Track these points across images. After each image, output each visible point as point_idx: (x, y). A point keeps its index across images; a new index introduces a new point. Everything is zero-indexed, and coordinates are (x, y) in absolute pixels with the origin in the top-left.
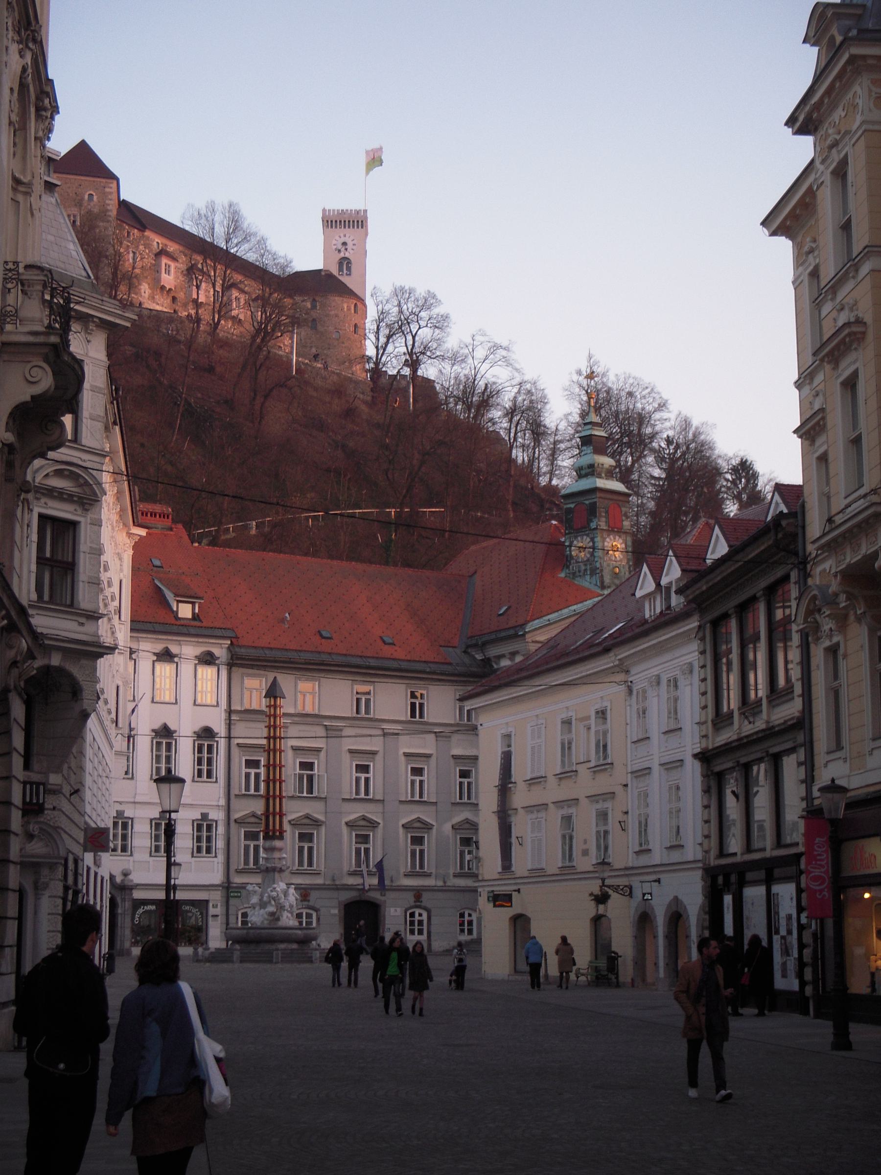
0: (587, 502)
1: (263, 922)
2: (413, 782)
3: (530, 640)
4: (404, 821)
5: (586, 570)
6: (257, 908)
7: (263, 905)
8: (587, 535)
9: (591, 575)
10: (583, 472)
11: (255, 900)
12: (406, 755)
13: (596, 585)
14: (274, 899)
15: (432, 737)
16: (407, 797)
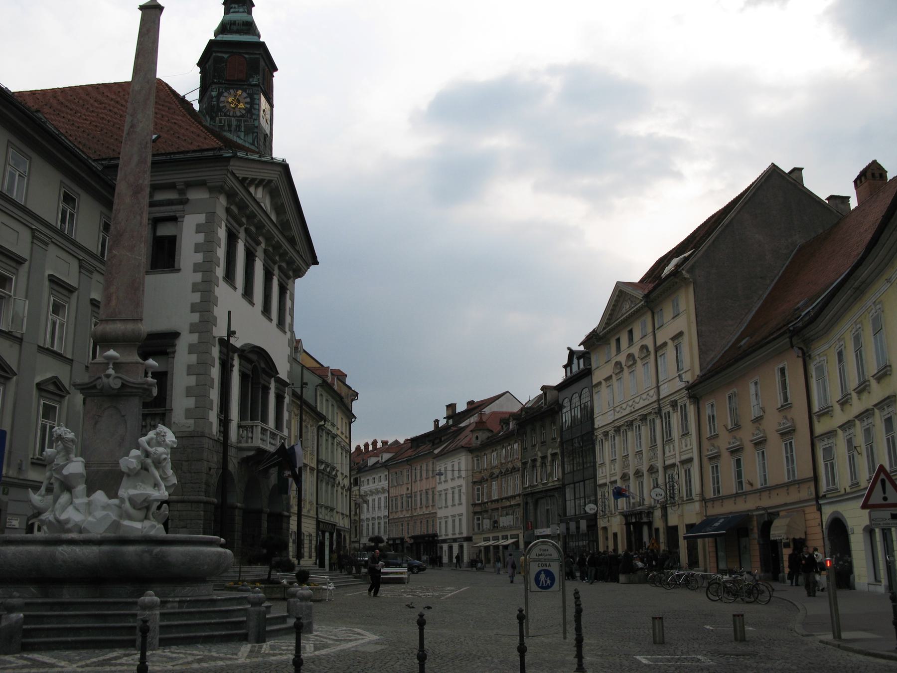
0: (246, 56)
1: (116, 525)
2: (54, 324)
3: (230, 168)
4: (38, 379)
5: (238, 127)
6: (81, 488)
7: (106, 479)
8: (244, 90)
9: (246, 134)
10: (235, 28)
11: (76, 466)
12: (53, 279)
13: (253, 144)
14: (158, 463)
15: (75, 264)
16: (45, 343)
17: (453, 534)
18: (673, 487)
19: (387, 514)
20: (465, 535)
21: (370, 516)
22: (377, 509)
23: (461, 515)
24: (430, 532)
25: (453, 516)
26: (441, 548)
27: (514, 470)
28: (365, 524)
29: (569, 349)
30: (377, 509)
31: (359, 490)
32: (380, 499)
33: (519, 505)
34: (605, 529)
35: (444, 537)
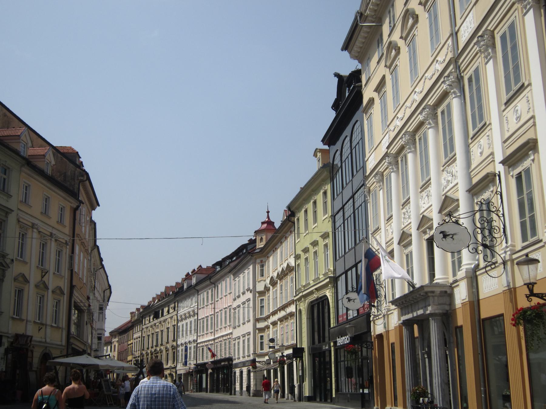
17: (244, 357)
18: (490, 222)
19: (195, 338)
20: (252, 357)
21: (183, 342)
22: (189, 332)
23: (249, 334)
24: (227, 356)
25: (244, 336)
26: (235, 373)
27: (290, 269)
28: (180, 349)
29: (337, 75)
30: (189, 332)
31: (177, 315)
32: (191, 322)
33: (291, 315)
34: (380, 337)
35: (234, 362)
